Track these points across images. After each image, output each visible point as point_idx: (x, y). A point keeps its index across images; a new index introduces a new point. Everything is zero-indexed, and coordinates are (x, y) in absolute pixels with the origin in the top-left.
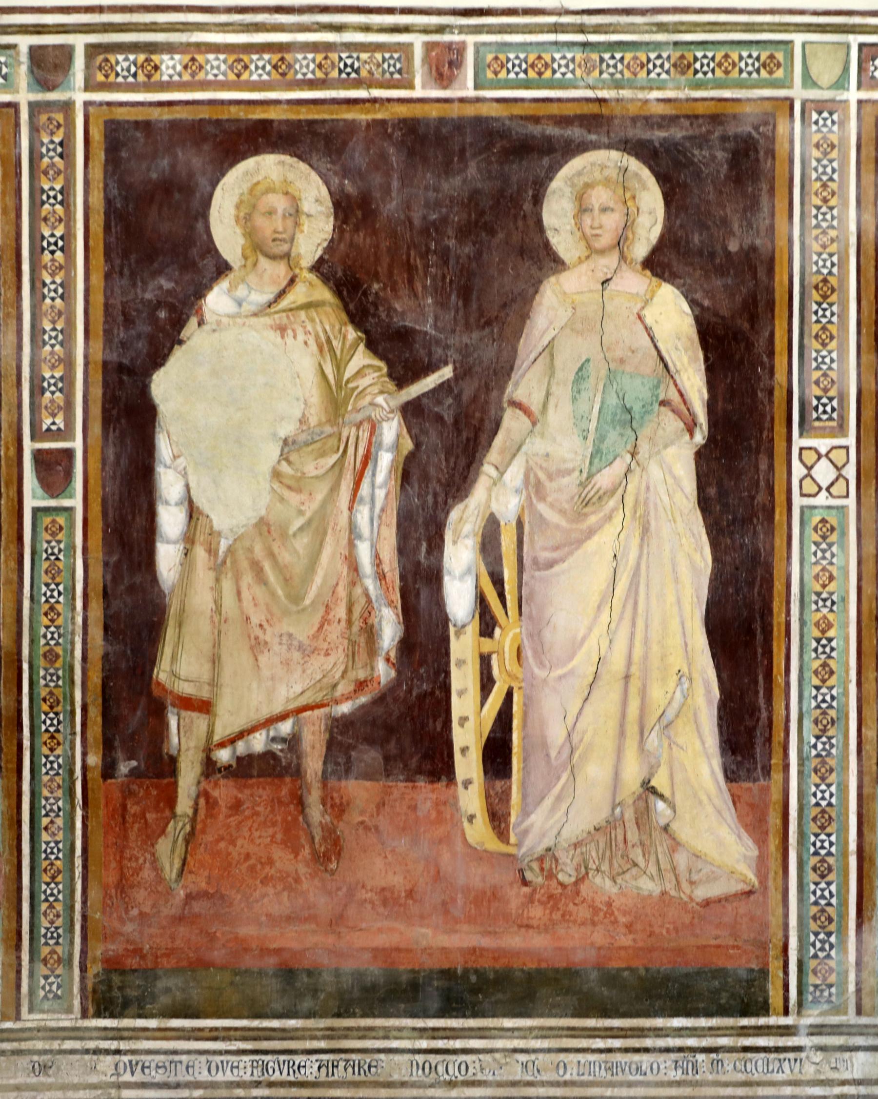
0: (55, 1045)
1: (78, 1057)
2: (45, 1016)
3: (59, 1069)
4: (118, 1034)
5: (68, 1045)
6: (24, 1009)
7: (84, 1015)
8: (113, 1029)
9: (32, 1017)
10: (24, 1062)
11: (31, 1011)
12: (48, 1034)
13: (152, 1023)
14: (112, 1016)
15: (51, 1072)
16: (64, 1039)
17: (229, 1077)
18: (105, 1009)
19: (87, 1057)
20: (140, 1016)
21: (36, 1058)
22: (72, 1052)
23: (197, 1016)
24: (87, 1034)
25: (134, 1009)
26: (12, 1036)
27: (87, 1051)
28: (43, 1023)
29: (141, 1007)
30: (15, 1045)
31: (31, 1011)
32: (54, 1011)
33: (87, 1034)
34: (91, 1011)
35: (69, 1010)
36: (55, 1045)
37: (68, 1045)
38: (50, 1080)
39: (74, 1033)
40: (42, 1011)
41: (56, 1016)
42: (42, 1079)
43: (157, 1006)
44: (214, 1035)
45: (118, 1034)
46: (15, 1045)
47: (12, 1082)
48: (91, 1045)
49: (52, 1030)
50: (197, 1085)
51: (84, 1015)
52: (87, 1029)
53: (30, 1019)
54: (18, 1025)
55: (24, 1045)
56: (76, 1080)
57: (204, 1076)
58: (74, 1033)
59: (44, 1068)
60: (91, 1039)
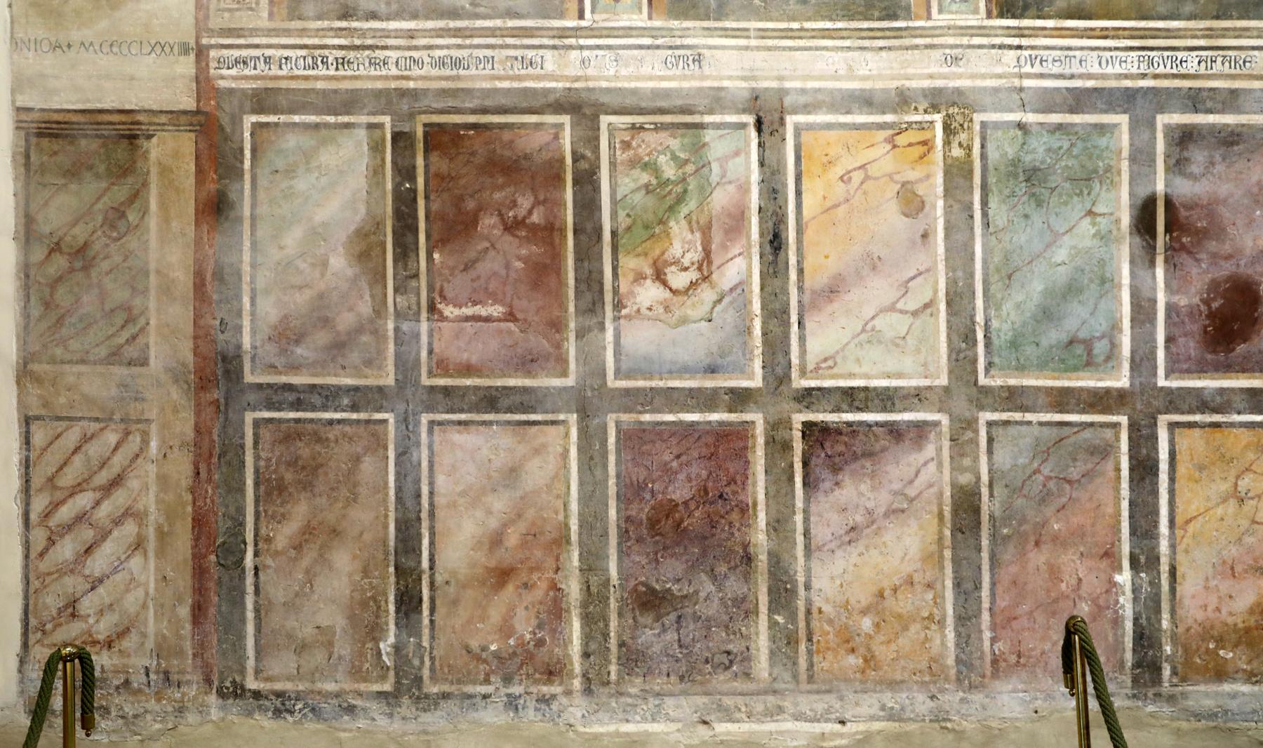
0: (965, 41)
1: (985, 51)
2: (953, 16)
3: (968, 61)
4: (1020, 33)
5: (977, 41)
6: (934, 10)
7: (989, 15)
8: (1014, 28)
9: (941, 17)
10: (937, 54)
11: (940, 11)
12: (958, 31)
13: (1050, 23)
14: (1014, 17)
15: (961, 63)
16: (972, 36)
17: (1118, 70)
18: (1008, 11)
19: (993, 51)
20: (1039, 17)
21: (948, 51)
22: (980, 47)
23: (1089, 17)
24: (992, 32)
25: (1033, 11)
26: (925, 33)
27: (993, 46)
28: (952, 23)
29: (1039, 10)
30: (928, 41)
31: (940, 11)
32: (962, 13)
33: (992, 32)
34: (995, 12)
35: (976, 11)
36: (965, 41)
37: (977, 41)
38: (960, 70)
39: (981, 31)
40: (951, 12)
41: (964, 16)
42: (954, 69)
43: (1054, 9)
44: (1104, 34)
45: (1020, 33)
46: (928, 41)
47: (926, 71)
48: (997, 41)
49: (961, 28)
50: (1090, 76)
51: (989, 15)
52: (992, 27)
53: (939, 19)
54: (930, 24)
55: (936, 41)
56: (983, 71)
57: (1096, 69)
58: (981, 31)
59: (956, 59)
60: (996, 36)
